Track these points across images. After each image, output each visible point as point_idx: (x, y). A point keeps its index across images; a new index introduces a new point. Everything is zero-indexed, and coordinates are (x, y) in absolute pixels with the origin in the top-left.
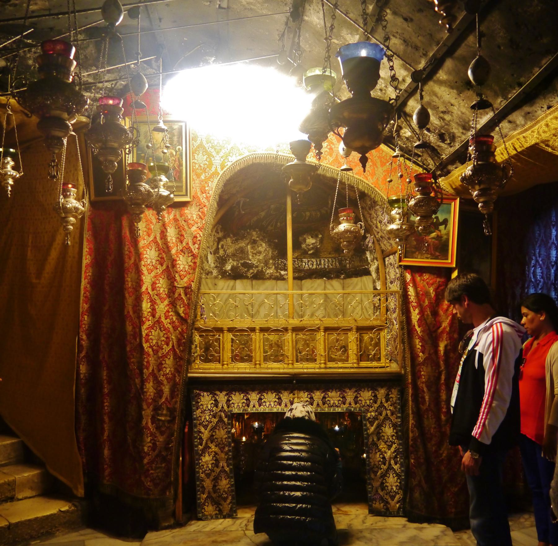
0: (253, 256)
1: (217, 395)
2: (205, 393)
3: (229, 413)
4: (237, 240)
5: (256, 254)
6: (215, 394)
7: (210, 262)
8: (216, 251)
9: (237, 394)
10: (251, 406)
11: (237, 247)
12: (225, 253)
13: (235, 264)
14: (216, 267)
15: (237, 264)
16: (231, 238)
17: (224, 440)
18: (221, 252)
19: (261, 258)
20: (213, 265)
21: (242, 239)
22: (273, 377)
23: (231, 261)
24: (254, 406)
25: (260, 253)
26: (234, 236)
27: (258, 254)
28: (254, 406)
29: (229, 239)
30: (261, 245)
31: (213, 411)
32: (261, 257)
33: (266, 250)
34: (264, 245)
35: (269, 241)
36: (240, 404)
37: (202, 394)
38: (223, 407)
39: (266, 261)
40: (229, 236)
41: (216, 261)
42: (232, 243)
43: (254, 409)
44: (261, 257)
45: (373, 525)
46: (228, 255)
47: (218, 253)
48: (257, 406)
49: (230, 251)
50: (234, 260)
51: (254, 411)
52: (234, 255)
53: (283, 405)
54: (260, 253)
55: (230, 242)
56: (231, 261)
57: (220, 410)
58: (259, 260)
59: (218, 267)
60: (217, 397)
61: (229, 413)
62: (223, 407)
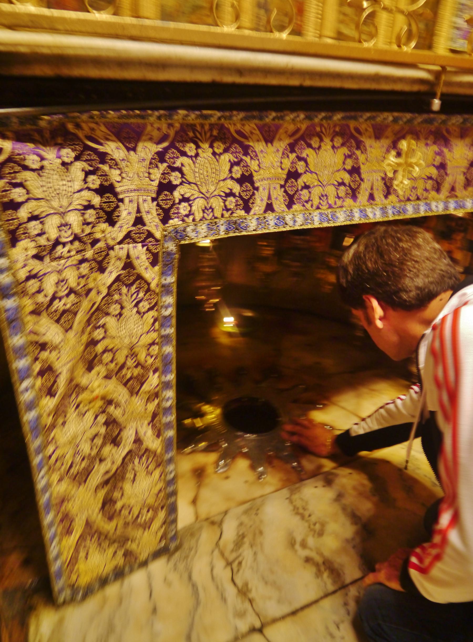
1: (115, 165)
2: (50, 154)
3: (171, 246)
6: (103, 157)
9: (206, 152)
10: (258, 206)
17: (142, 356)
22: (377, 78)
24: (269, 208)
28: (269, 208)
31: (95, 242)
36: (217, 204)
37: (32, 160)
38: (139, 221)
43: (270, 216)
48: (280, 205)
51: (272, 227)
53: (363, 197)
57: (128, 236)
60: (114, 175)
61: (171, 246)
62: (139, 221)
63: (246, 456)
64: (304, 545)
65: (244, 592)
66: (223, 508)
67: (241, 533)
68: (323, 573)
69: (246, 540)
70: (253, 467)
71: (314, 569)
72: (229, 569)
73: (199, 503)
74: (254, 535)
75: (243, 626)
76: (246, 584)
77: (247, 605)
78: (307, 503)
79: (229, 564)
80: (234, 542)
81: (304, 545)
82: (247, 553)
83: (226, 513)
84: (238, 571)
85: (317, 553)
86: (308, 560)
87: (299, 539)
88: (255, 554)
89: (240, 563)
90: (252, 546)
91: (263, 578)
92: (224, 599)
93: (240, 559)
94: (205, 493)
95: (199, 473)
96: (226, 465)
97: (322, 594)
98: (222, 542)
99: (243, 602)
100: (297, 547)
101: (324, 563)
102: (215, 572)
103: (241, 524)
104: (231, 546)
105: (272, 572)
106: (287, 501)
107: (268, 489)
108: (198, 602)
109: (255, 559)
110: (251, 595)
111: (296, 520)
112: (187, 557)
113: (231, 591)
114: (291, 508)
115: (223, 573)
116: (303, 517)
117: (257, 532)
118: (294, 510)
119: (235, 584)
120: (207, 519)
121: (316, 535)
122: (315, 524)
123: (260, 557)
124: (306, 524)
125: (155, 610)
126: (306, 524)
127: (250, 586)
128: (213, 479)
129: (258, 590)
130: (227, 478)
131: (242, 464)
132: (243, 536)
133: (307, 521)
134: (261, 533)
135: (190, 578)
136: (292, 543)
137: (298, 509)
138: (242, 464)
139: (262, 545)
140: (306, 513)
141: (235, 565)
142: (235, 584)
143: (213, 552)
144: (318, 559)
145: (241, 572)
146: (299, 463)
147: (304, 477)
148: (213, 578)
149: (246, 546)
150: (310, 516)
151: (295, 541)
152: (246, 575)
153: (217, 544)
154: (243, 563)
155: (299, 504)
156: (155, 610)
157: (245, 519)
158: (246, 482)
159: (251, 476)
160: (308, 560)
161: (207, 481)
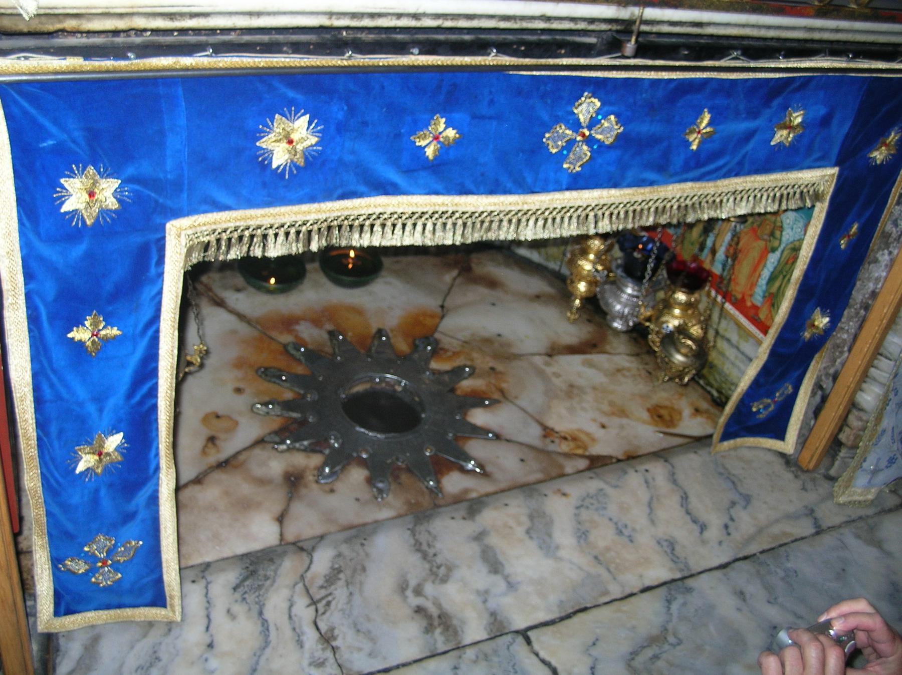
45: (736, 536)
63: (363, 463)
64: (418, 592)
65: (327, 639)
66: (318, 530)
67: (336, 566)
68: (436, 628)
69: (341, 576)
70: (370, 481)
71: (424, 623)
72: (313, 608)
73: (286, 522)
74: (355, 571)
76: (332, 629)
77: (329, 654)
78: (435, 538)
79: (314, 602)
80: (325, 577)
81: (418, 592)
82: (340, 592)
83: (322, 537)
84: (324, 613)
85: (434, 604)
86: (419, 610)
87: (413, 583)
88: (351, 594)
89: (328, 604)
90: (348, 584)
91: (355, 625)
92: (300, 644)
93: (330, 598)
94: (297, 508)
95: (293, 481)
96: (332, 473)
97: (429, 654)
98: (309, 575)
99: (323, 650)
100: (409, 593)
101: (439, 617)
102: (295, 610)
103: (339, 555)
104: (320, 582)
105: (369, 619)
106: (409, 532)
107: (385, 514)
108: (267, 643)
109: (349, 602)
110: (334, 644)
111: (414, 559)
112: (260, 587)
113: (310, 636)
114: (412, 541)
115: (303, 611)
116: (425, 556)
117: (359, 567)
118: (415, 545)
119: (318, 629)
120: (294, 544)
121: (438, 581)
122: (439, 567)
123: (357, 599)
124: (427, 566)
125: (210, 646)
126: (427, 566)
127: (336, 632)
128: (312, 490)
129: (345, 639)
130: (332, 491)
131: (357, 475)
132: (339, 571)
133: (429, 562)
134: (364, 569)
135: (261, 613)
136: (402, 588)
137: (421, 544)
138: (357, 475)
139: (361, 583)
140: (431, 552)
141: (320, 606)
142: (318, 629)
143: (295, 585)
144: (434, 611)
145: (328, 614)
146: (438, 482)
147: (441, 502)
148: (290, 617)
149: (341, 583)
150: (435, 555)
151: (407, 586)
152: (333, 619)
153: (302, 577)
154: (333, 603)
155: (423, 538)
156: (210, 646)
157: (345, 549)
158: (357, 500)
159: (365, 493)
160: (419, 610)
161: (303, 491)
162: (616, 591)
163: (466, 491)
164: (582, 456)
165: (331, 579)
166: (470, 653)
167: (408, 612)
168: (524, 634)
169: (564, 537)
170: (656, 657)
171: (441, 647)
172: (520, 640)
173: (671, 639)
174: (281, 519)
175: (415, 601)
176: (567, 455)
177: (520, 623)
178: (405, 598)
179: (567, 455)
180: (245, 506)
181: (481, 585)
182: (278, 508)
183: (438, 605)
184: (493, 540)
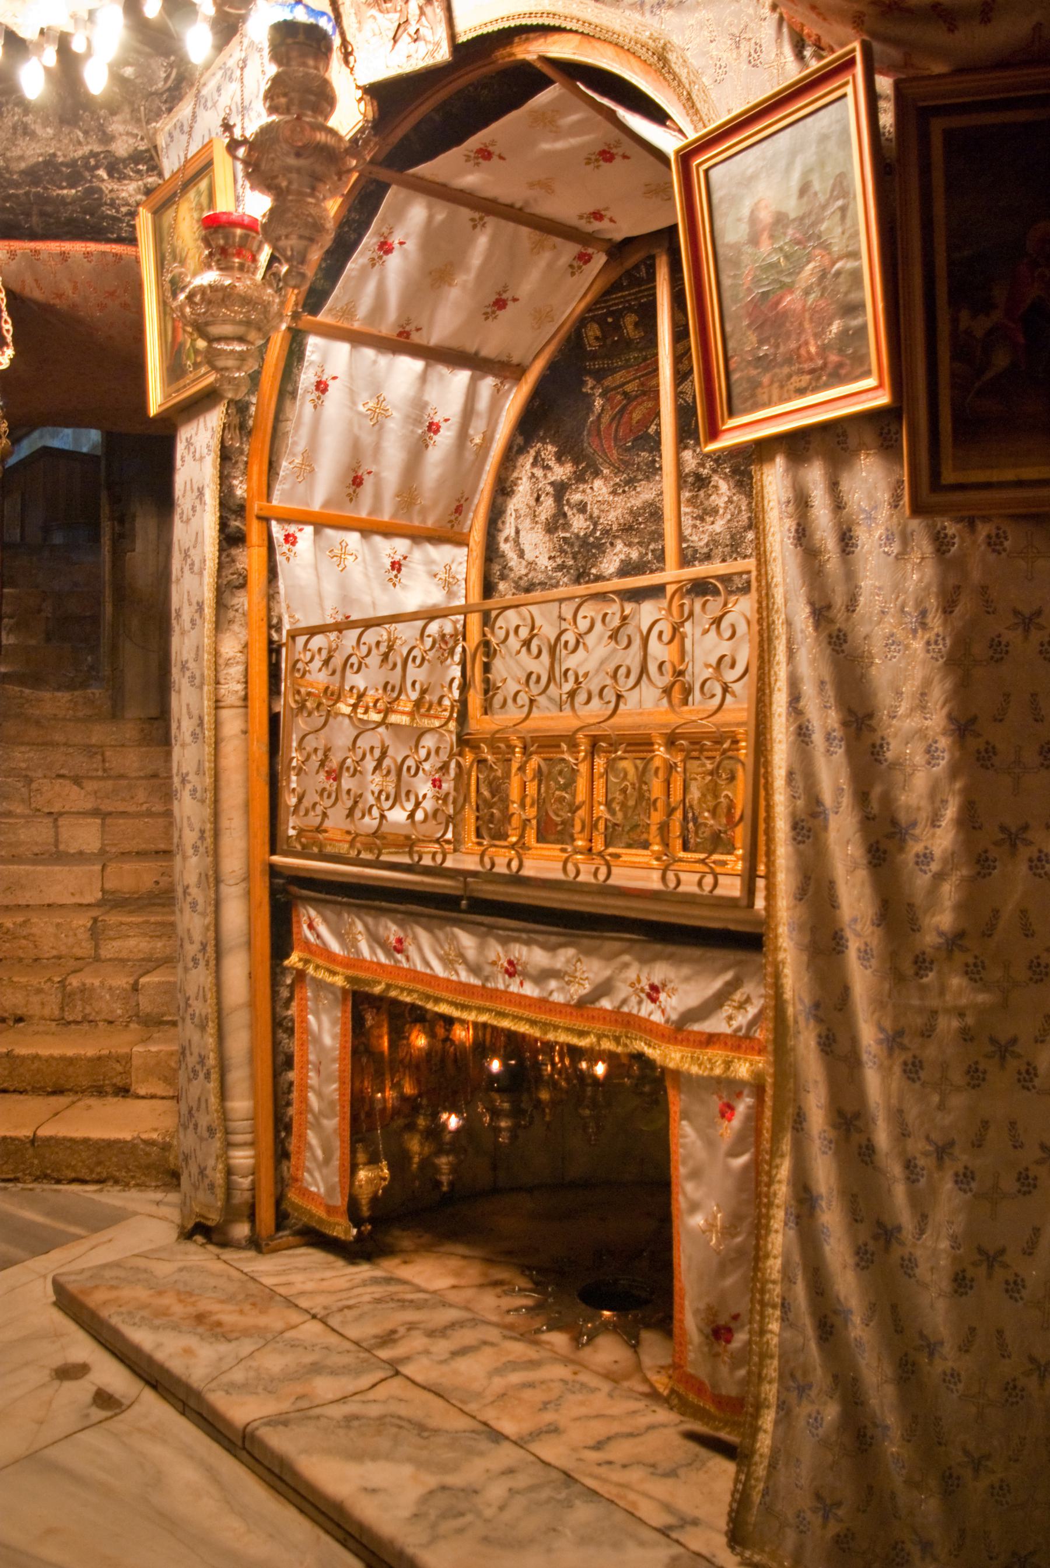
0: (695, 526)
4: (630, 482)
5: (702, 520)
7: (529, 556)
8: (555, 524)
11: (636, 502)
12: (595, 524)
13: (634, 555)
14: (561, 567)
15: (642, 556)
16: (606, 479)
18: (579, 524)
19: (718, 530)
20: (543, 562)
21: (648, 478)
23: (619, 545)
25: (714, 511)
26: (617, 471)
27: (709, 519)
29: (598, 483)
30: (716, 487)
32: (719, 525)
33: (730, 501)
34: (723, 486)
35: (735, 471)
39: (732, 537)
40: (597, 473)
41: (562, 551)
42: (614, 493)
44: (719, 525)
46: (606, 532)
47: (567, 526)
49: (613, 517)
50: (630, 545)
52: (627, 529)
54: (714, 511)
55: (604, 490)
56: (619, 545)
58: (714, 542)
59: (570, 568)
64: (409, 1329)
75: (313, 1312)
82: (392, 1305)
144: (396, 1336)
162: (472, 1407)
163: (548, 1343)
164: (652, 1386)
165: (403, 1301)
166: (364, 1355)
167: (389, 1326)
168: (397, 1373)
169: (516, 1378)
170: (400, 1427)
171: (364, 1344)
172: (390, 1373)
173: (426, 1434)
174: (454, 1287)
175: (402, 1330)
176: (646, 1380)
177: (407, 1370)
178: (403, 1325)
179: (646, 1380)
180: (457, 1274)
181: (433, 1349)
182: (463, 1282)
183: (403, 1337)
184: (488, 1351)
